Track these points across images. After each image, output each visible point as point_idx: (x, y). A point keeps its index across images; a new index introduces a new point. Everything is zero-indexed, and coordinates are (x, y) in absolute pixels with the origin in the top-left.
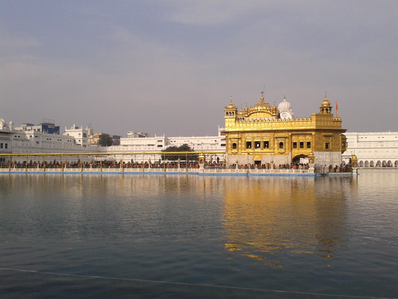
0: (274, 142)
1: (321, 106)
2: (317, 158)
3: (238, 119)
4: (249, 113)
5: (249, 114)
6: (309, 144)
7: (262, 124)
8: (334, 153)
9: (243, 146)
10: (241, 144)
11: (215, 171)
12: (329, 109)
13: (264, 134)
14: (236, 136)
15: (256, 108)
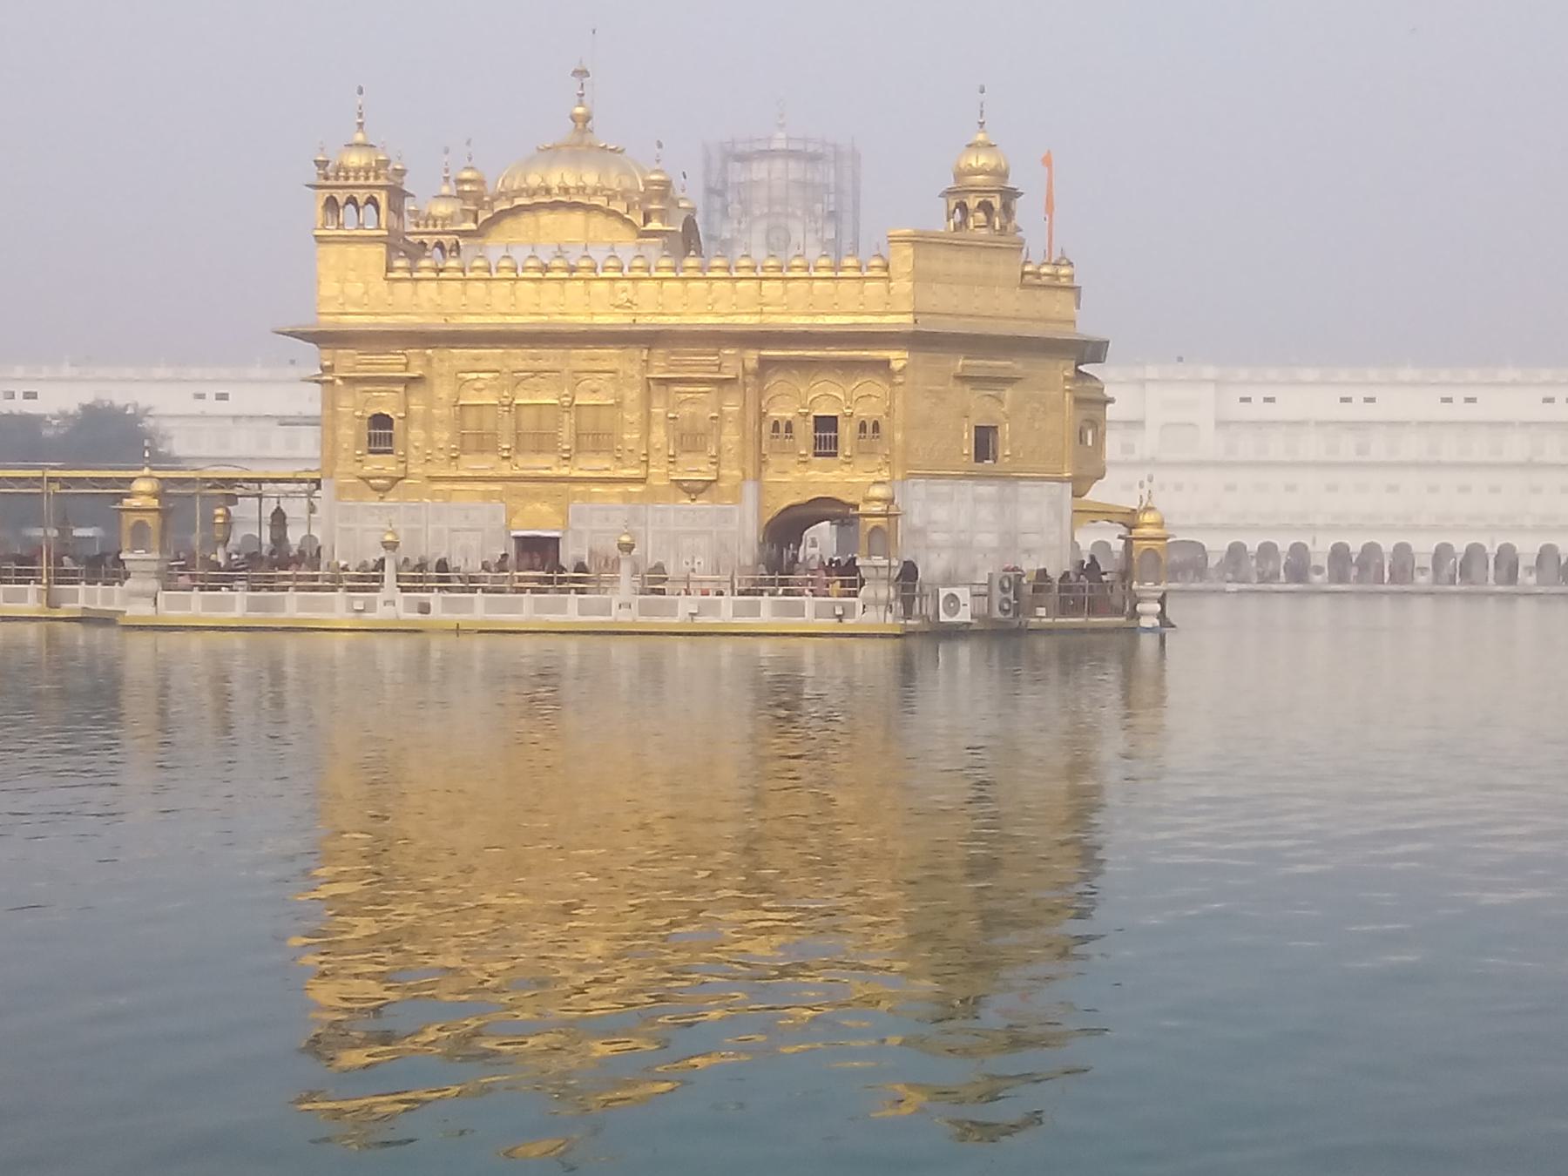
0: (649, 412)
1: (951, 184)
2: (916, 520)
3: (416, 252)
4: (488, 212)
5: (484, 216)
6: (870, 429)
7: (569, 284)
8: (1025, 489)
9: (436, 435)
10: (428, 424)
11: (237, 604)
12: (997, 202)
13: (580, 357)
14: (392, 363)
15: (534, 180)
